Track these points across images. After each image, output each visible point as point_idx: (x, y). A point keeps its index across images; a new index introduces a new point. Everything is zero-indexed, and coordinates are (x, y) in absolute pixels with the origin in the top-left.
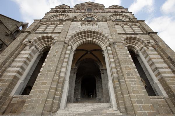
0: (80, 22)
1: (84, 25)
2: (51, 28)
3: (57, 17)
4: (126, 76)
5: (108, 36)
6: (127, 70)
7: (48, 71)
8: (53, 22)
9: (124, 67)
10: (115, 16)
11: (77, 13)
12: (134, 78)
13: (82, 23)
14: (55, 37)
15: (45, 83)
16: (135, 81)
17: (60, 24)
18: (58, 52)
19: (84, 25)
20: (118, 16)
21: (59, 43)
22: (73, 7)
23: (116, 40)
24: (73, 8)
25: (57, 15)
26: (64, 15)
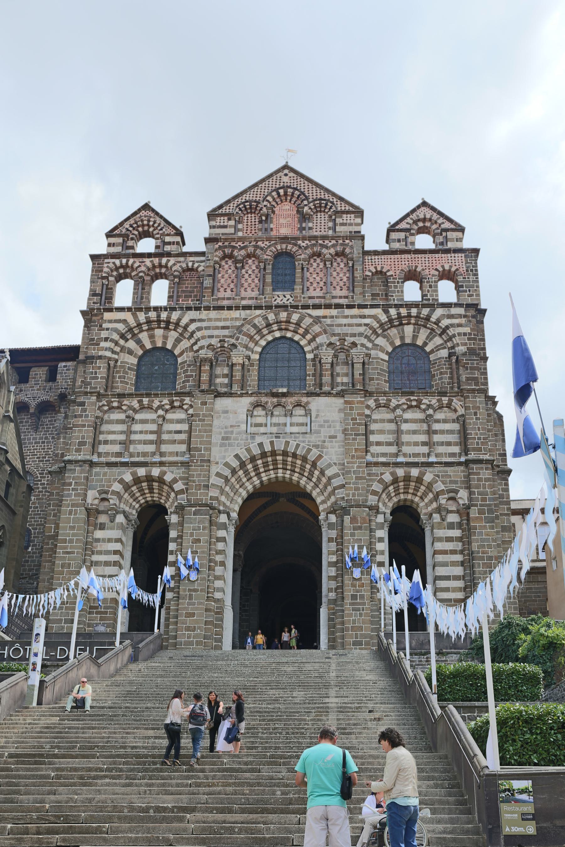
0: (246, 402)
1: (259, 412)
2: (146, 432)
3: (141, 336)
4: (348, 601)
5: (336, 475)
6: (353, 585)
7: (190, 590)
8: (146, 401)
9: (349, 581)
10: (395, 326)
11: (226, 312)
12: (364, 604)
13: (252, 404)
14: (175, 481)
15: (193, 615)
16: (363, 610)
17: (173, 407)
18: (199, 541)
19: (260, 408)
20: (408, 324)
21: (194, 509)
22: (202, 247)
23: (354, 495)
24: (203, 254)
25: (139, 325)
26: (168, 322)
